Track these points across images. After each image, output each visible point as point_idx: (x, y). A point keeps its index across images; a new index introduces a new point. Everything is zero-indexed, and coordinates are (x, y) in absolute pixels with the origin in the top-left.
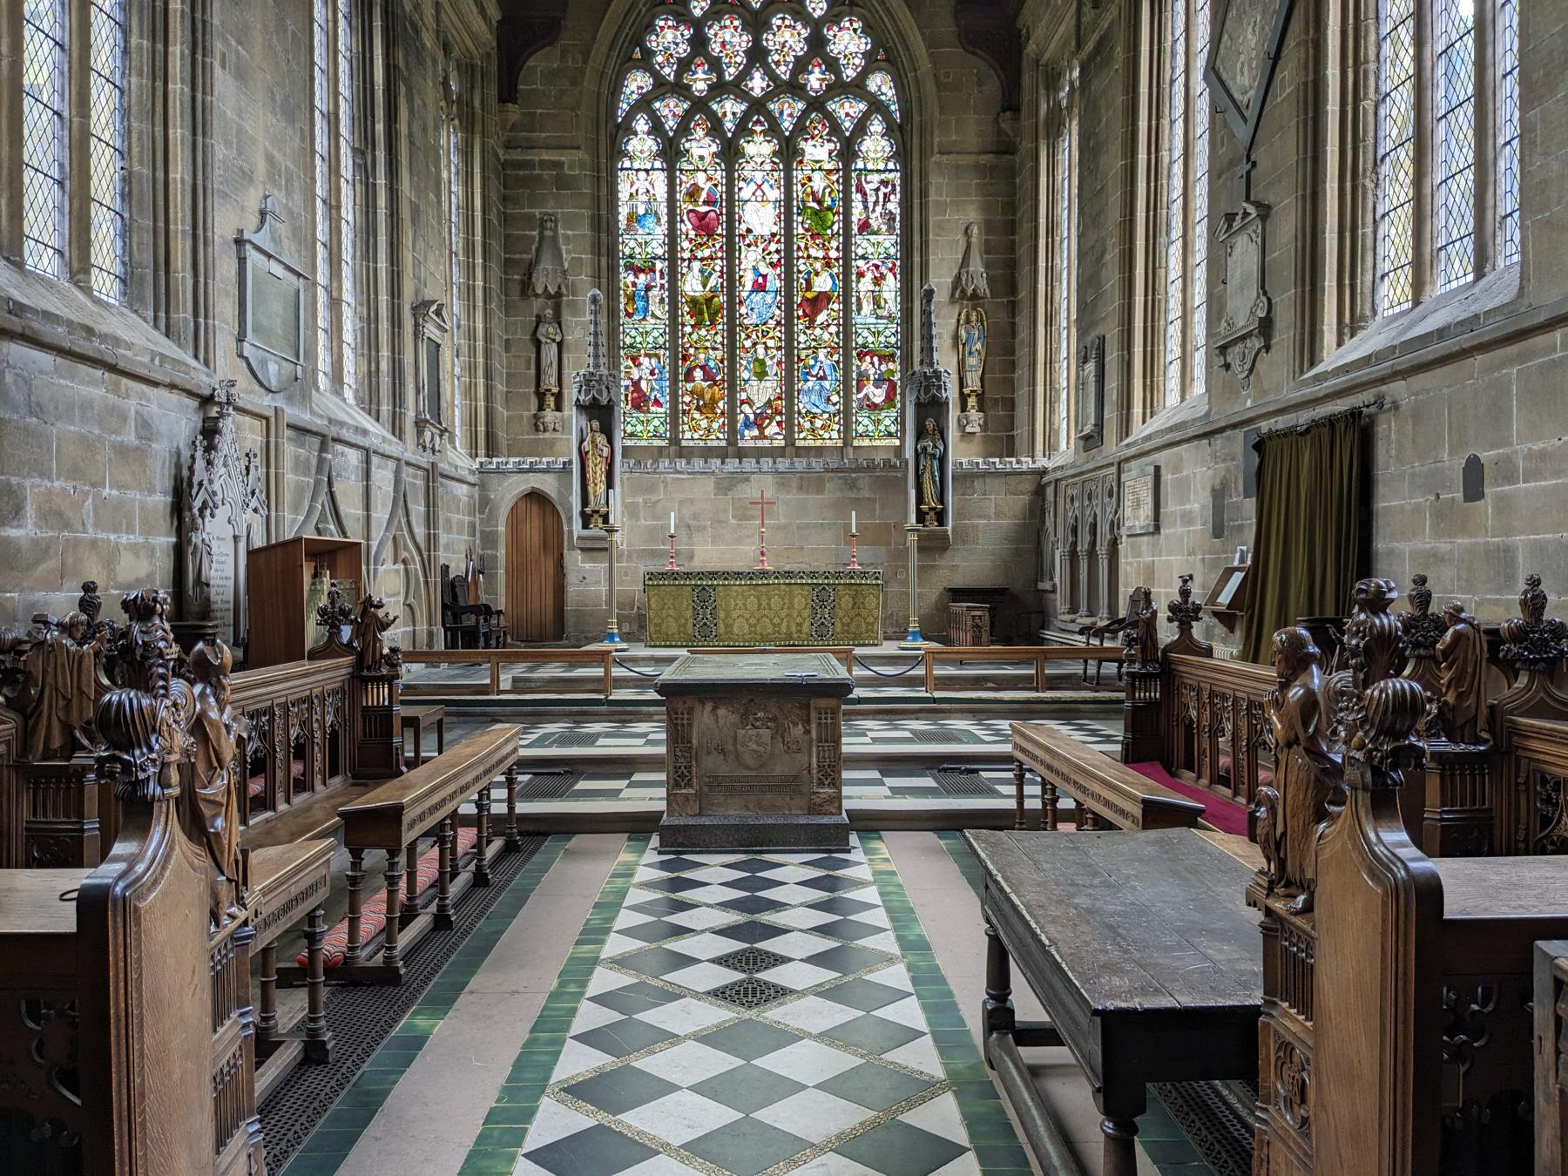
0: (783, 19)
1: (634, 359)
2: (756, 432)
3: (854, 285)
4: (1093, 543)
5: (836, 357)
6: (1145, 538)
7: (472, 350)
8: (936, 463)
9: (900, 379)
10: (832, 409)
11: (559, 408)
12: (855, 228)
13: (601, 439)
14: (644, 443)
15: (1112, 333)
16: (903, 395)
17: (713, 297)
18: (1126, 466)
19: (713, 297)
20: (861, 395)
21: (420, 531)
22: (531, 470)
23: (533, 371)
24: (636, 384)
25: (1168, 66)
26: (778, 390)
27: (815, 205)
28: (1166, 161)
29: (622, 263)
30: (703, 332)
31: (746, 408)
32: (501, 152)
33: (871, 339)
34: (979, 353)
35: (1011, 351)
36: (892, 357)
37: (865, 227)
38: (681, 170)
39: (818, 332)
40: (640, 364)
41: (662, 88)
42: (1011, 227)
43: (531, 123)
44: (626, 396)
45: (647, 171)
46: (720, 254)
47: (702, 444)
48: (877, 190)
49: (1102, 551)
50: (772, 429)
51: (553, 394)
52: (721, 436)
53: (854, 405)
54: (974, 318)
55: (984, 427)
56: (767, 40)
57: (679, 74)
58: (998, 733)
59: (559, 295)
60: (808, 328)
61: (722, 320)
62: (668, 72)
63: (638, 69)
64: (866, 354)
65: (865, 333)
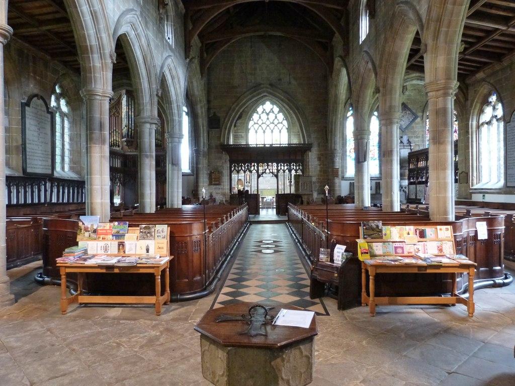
41: (255, 123)
43: (237, 130)
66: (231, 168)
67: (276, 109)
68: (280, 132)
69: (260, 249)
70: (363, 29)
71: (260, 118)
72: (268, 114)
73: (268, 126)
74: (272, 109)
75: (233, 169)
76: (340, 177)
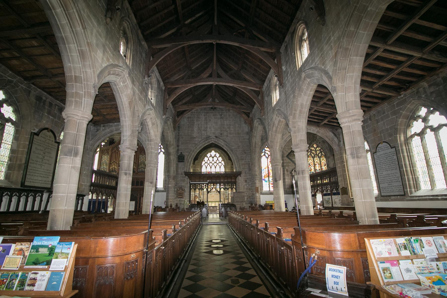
41: (206, 163)
43: (196, 166)
66: (190, 187)
67: (218, 155)
68: (220, 168)
69: (211, 249)
70: (274, 98)
71: (209, 159)
72: (213, 158)
73: (213, 164)
74: (215, 155)
75: (192, 187)
76: (259, 192)
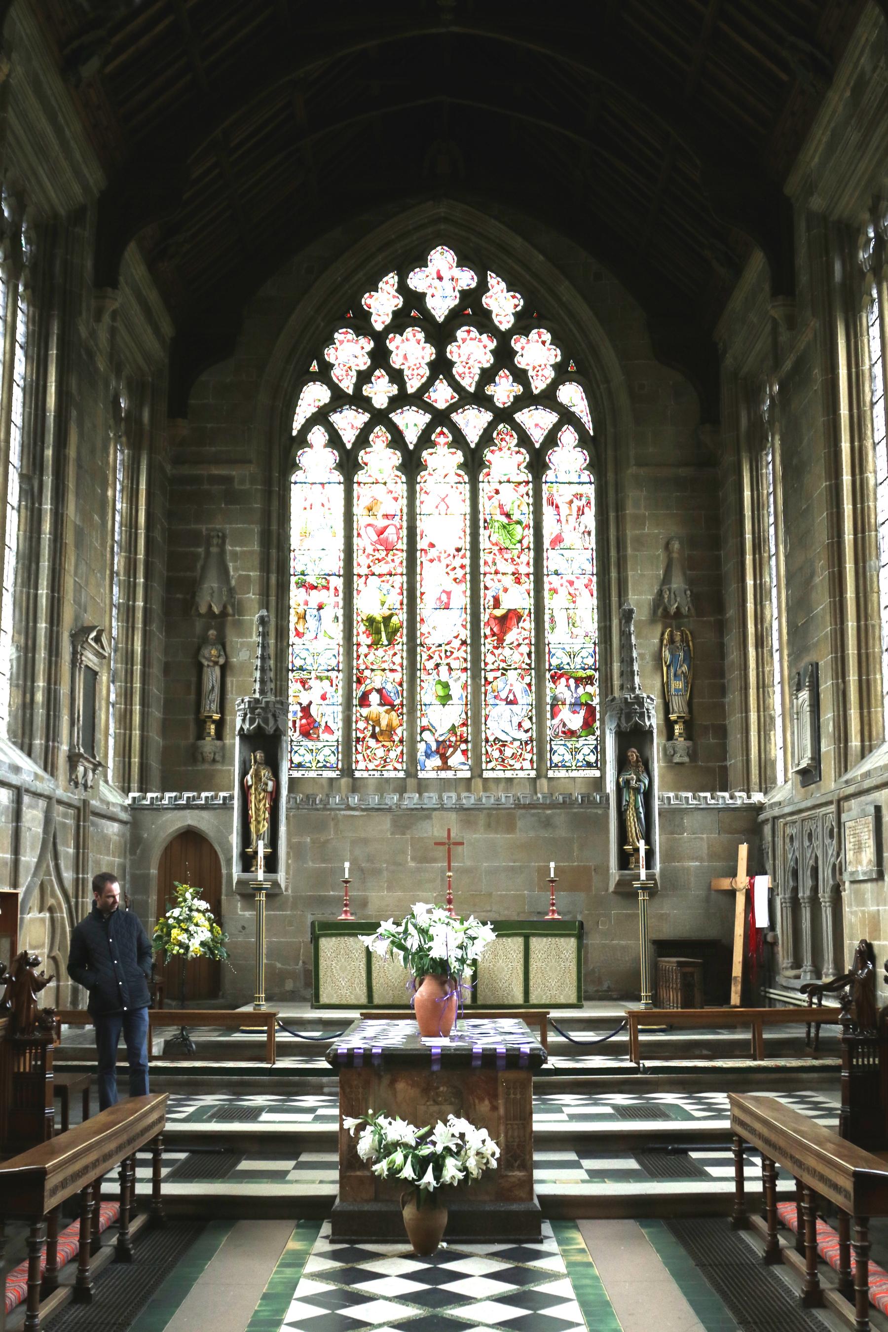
0: (469, 332)
1: (303, 682)
2: (436, 761)
3: (546, 601)
4: (815, 889)
5: (527, 679)
6: (869, 886)
7: (130, 673)
8: (640, 798)
9: (600, 704)
10: (525, 737)
11: (219, 736)
12: (546, 544)
13: (265, 773)
14: (313, 774)
15: (825, 661)
16: (602, 721)
17: (391, 616)
18: (846, 805)
19: (391, 616)
20: (556, 721)
21: (68, 875)
22: (188, 806)
23: (193, 697)
24: (306, 710)
25: (867, 389)
26: (464, 716)
27: (504, 520)
28: (872, 482)
29: (293, 580)
30: (380, 652)
31: (426, 735)
32: (168, 468)
33: (566, 660)
34: (686, 677)
35: (720, 672)
36: (589, 680)
37: (557, 540)
38: (359, 483)
39: (507, 652)
40: (310, 688)
41: (339, 399)
42: (715, 542)
44: (294, 722)
45: (323, 484)
46: (399, 570)
47: (377, 774)
48: (571, 502)
49: (824, 897)
50: (456, 759)
51: (214, 722)
52: (399, 766)
53: (549, 732)
54: (678, 638)
55: (693, 755)
56: (451, 352)
57: (358, 387)
58: (710, 1107)
59: (224, 614)
60: (496, 648)
61: (402, 638)
62: (348, 385)
63: (314, 381)
64: (561, 676)
65: (559, 653)
